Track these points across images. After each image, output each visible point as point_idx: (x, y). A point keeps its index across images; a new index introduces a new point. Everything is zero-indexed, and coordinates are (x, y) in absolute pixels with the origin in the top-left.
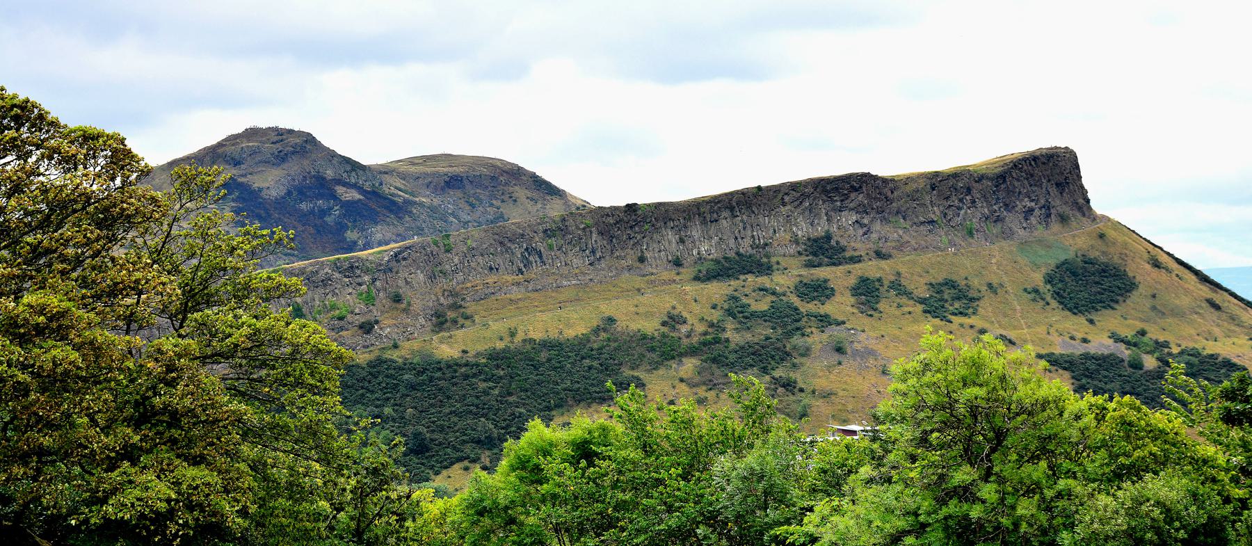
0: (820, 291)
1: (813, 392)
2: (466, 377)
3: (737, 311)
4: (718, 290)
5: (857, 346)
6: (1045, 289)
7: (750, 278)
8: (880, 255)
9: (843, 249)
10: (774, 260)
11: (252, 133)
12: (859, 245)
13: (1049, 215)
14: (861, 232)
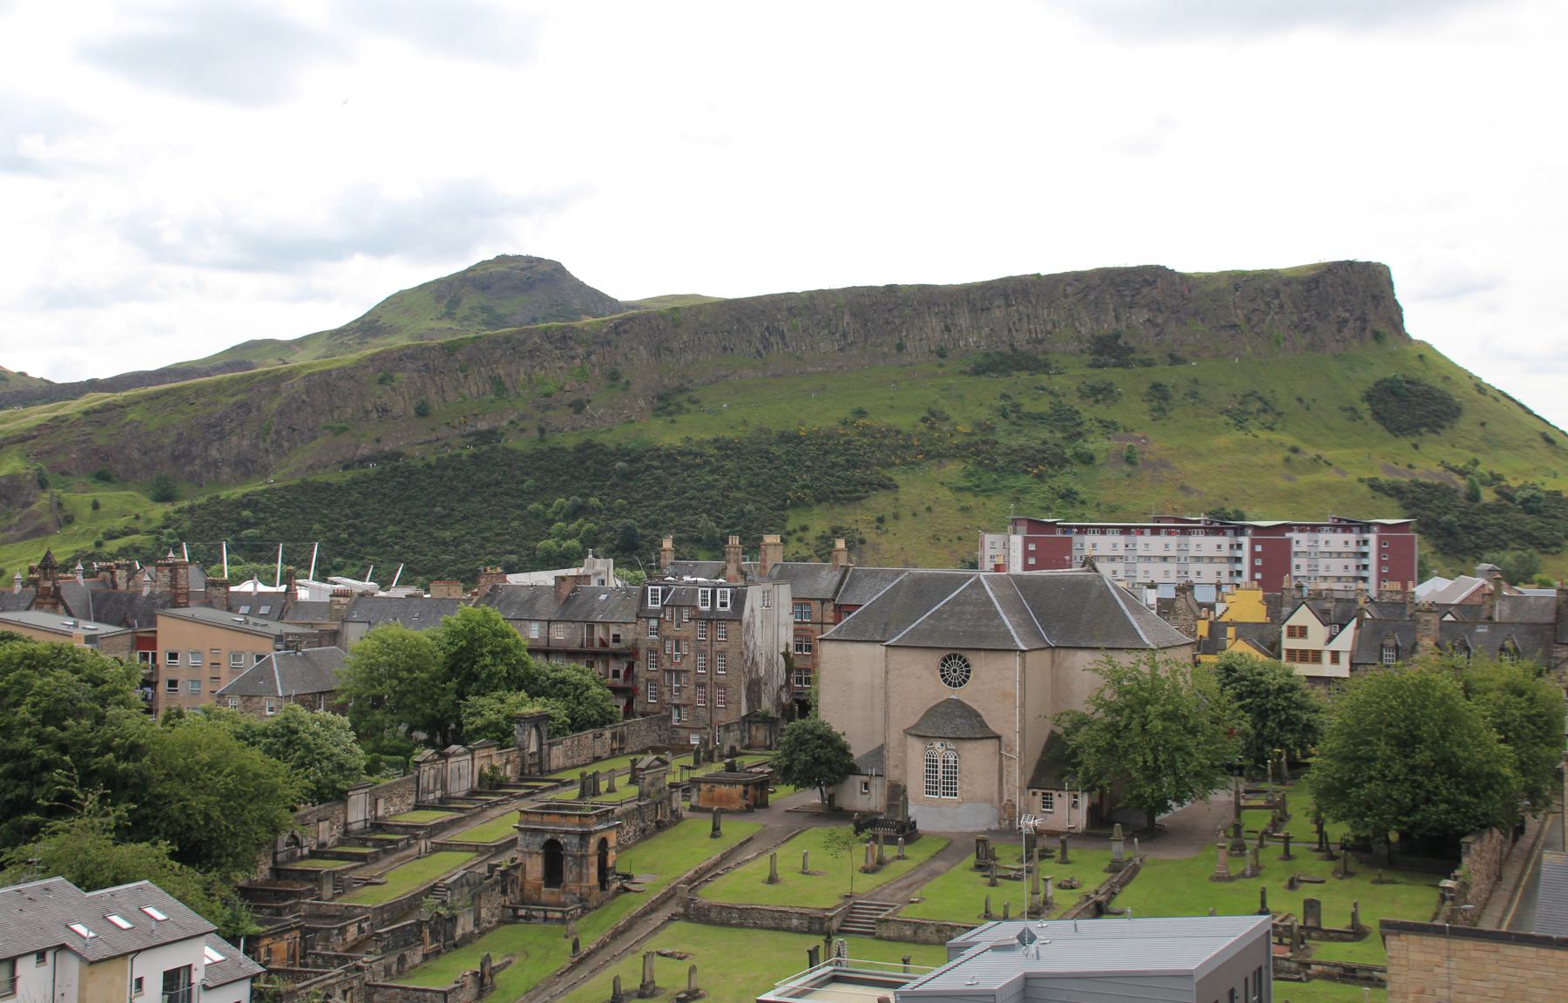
2: (688, 467)
3: (1011, 413)
7: (1025, 375)
8: (1174, 360)
9: (1132, 350)
13: (1364, 329)
14: (1152, 332)
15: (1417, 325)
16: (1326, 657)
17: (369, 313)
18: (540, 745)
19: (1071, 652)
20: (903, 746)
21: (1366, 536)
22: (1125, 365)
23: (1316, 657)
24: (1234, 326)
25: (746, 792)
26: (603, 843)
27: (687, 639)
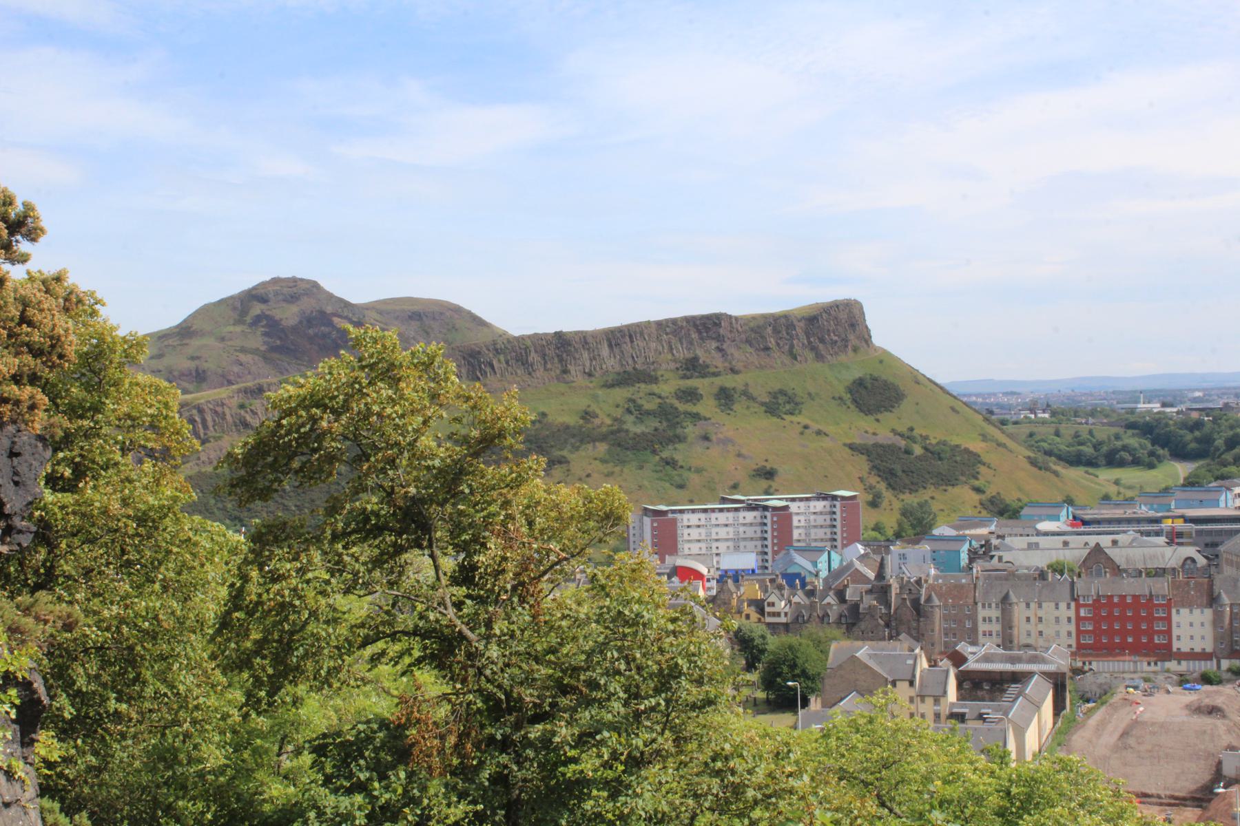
0: (691, 395)
1: (690, 469)
3: (633, 408)
4: (620, 394)
5: (720, 436)
6: (847, 397)
7: (643, 386)
8: (733, 371)
9: (708, 366)
10: (659, 373)
11: (275, 281)
12: (718, 362)
13: (846, 346)
15: (877, 340)
17: (185, 321)
22: (703, 376)
23: (778, 614)
24: (767, 349)
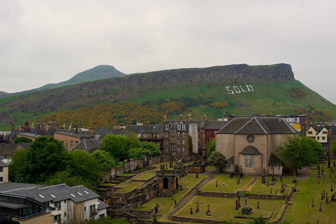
11: (101, 66)
13: (287, 78)
14: (244, 78)
15: (296, 77)
16: (316, 138)
18: (147, 160)
19: (276, 135)
20: (238, 156)
21: (297, 118)
24: (261, 77)
25: (201, 168)
26: (177, 178)
27: (175, 136)
